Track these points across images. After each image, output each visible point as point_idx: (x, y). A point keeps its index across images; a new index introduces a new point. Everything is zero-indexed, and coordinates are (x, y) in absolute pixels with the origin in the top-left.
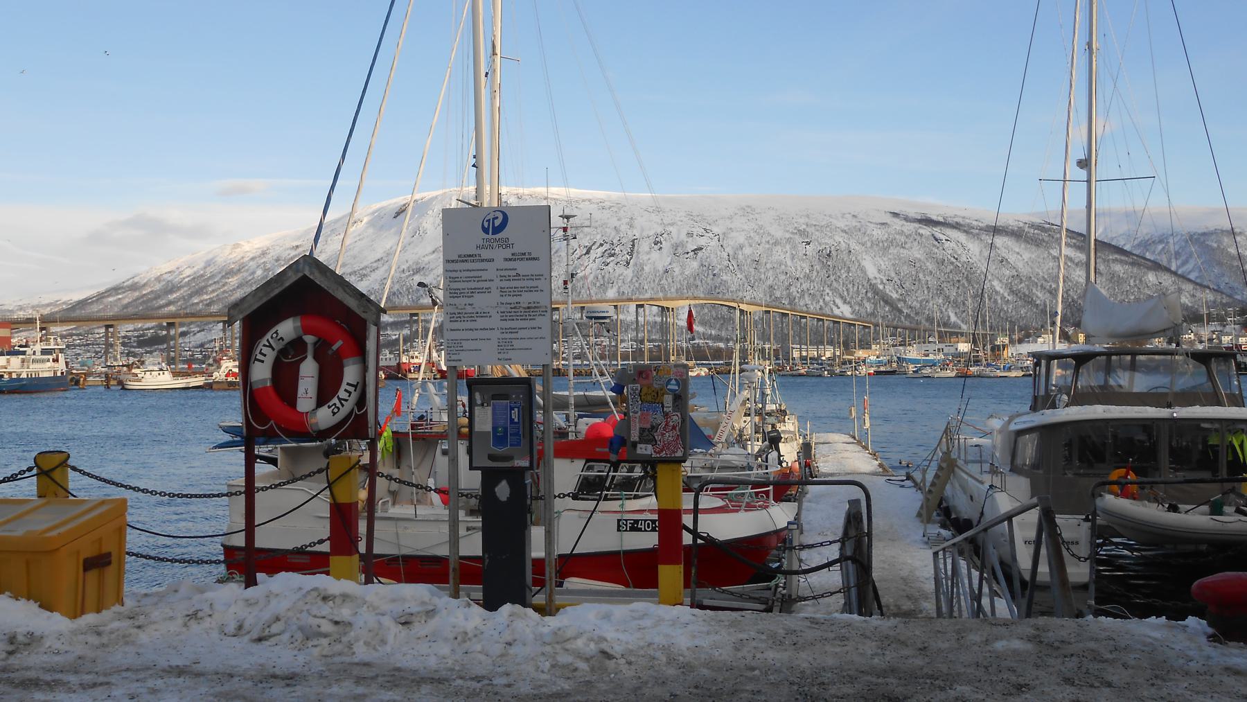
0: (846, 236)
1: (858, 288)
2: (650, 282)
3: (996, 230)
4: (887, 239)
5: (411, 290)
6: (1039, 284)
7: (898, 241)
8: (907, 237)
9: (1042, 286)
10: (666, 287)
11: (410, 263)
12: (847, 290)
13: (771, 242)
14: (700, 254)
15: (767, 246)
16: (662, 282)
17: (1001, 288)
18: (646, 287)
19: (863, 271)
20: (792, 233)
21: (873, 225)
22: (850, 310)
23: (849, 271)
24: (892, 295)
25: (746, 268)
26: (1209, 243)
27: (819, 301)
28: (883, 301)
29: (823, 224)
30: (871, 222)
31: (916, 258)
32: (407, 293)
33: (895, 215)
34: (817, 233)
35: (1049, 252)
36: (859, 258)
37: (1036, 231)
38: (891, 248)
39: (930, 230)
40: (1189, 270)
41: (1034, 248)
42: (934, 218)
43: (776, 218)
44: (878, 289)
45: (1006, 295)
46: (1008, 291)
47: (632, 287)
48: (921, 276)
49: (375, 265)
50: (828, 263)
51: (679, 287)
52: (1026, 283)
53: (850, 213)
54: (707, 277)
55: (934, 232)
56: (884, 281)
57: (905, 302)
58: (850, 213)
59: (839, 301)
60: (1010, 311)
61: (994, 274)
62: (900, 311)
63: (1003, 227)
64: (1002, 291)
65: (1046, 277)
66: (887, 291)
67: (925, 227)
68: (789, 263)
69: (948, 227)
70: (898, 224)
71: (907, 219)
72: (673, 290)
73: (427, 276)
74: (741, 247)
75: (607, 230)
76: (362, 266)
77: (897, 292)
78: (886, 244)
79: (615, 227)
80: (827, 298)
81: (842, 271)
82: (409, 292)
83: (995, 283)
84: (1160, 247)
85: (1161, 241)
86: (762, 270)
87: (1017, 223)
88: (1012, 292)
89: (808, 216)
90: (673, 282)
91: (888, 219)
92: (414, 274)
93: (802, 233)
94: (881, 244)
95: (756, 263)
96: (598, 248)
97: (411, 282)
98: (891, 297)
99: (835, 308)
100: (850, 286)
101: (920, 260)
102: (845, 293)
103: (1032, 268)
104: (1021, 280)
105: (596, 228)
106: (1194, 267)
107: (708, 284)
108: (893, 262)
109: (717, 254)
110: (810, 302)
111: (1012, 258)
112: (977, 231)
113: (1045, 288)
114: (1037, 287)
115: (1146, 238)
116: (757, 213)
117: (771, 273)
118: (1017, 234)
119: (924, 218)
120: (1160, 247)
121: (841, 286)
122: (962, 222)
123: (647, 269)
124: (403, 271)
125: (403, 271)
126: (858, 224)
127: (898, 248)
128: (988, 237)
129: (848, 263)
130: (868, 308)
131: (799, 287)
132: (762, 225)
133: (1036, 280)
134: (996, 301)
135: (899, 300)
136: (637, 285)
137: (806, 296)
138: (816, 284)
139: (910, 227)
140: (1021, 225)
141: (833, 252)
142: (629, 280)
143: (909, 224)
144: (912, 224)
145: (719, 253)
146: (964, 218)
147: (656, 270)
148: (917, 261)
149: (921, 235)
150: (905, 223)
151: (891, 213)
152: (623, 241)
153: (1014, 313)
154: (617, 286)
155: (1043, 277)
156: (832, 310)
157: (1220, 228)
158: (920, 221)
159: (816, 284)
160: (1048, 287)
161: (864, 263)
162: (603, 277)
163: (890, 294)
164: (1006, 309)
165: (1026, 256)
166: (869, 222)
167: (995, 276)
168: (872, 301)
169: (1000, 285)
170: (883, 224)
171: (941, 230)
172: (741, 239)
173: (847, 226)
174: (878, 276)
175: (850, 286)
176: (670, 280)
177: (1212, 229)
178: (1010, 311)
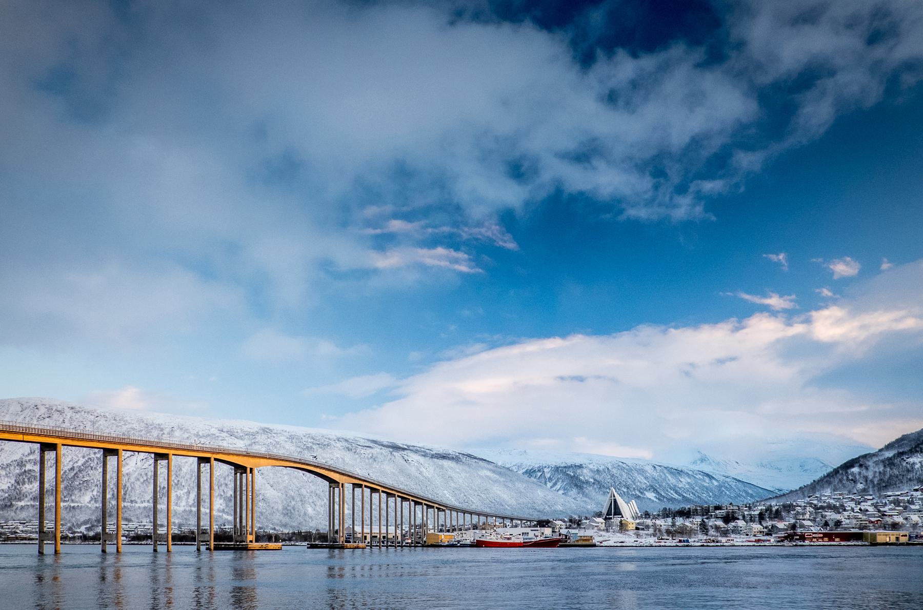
18: (183, 484)
21: (360, 447)
26: (569, 472)
30: (359, 445)
35: (477, 473)
40: (558, 489)
42: (401, 446)
58: (343, 438)
84: (539, 474)
85: (539, 471)
106: (560, 488)
115: (530, 469)
116: (274, 433)
120: (539, 474)
123: (184, 470)
136: (176, 481)
140: (457, 454)
157: (574, 464)
165: (464, 475)
173: (341, 446)
177: (569, 464)
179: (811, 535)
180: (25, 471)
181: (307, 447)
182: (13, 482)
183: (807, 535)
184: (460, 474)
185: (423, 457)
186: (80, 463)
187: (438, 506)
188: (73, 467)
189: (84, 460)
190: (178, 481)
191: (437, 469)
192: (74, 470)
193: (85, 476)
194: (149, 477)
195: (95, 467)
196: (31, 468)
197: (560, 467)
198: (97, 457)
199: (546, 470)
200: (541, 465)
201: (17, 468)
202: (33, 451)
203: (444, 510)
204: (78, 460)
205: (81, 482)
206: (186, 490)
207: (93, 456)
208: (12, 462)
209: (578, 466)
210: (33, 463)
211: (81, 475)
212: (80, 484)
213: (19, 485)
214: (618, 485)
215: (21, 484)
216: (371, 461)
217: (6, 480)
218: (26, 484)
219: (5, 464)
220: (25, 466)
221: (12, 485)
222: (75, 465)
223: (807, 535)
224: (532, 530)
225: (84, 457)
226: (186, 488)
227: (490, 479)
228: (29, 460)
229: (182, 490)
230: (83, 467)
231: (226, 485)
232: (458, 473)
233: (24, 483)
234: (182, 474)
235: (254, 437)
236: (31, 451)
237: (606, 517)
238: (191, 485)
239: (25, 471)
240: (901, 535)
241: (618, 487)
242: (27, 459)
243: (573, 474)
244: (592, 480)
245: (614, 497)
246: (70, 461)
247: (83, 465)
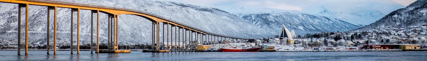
18: (85, 23)
21: (166, 5)
26: (263, 17)
40: (258, 25)
42: (186, 5)
58: (159, 1)
84: (250, 18)
85: (249, 16)
87: (210, 8)
106: (259, 24)
115: (245, 15)
120: (250, 18)
136: (81, 21)
140: (212, 9)
157: (265, 13)
165: (214, 18)
173: (158, 5)
177: (263, 13)
179: (375, 46)
180: (12, 16)
181: (142, 5)
182: (6, 21)
183: (373, 46)
185: (196, 10)
186: (37, 13)
187: (202, 33)
188: (34, 14)
189: (39, 11)
190: (83, 21)
192: (34, 16)
193: (39, 19)
194: (69, 19)
195: (44, 14)
196: (14, 15)
197: (259, 15)
198: (45, 10)
199: (253, 16)
200: (250, 14)
201: (8, 15)
202: (15, 7)
203: (205, 35)
204: (36, 11)
205: (38, 22)
206: (86, 25)
207: (43, 9)
208: (5, 12)
209: (267, 14)
210: (15, 13)
211: (37, 18)
212: (37, 22)
213: (9, 23)
214: (286, 23)
215: (10, 22)
216: (171, 12)
218: (12, 23)
219: (2, 13)
220: (12, 14)
221: (6, 23)
222: (35, 14)
223: (373, 46)
224: (246, 44)
225: (39, 10)
226: (86, 24)
227: (227, 20)
228: (14, 12)
229: (84, 25)
230: (38, 15)
231: (105, 23)
232: (212, 17)
233: (11, 22)
234: (84, 18)
236: (14, 7)
237: (280, 38)
238: (89, 23)
239: (12, 16)
240: (417, 46)
241: (286, 24)
242: (13, 11)
243: (265, 18)
244: (274, 21)
245: (284, 28)
246: (32, 12)
247: (38, 14)
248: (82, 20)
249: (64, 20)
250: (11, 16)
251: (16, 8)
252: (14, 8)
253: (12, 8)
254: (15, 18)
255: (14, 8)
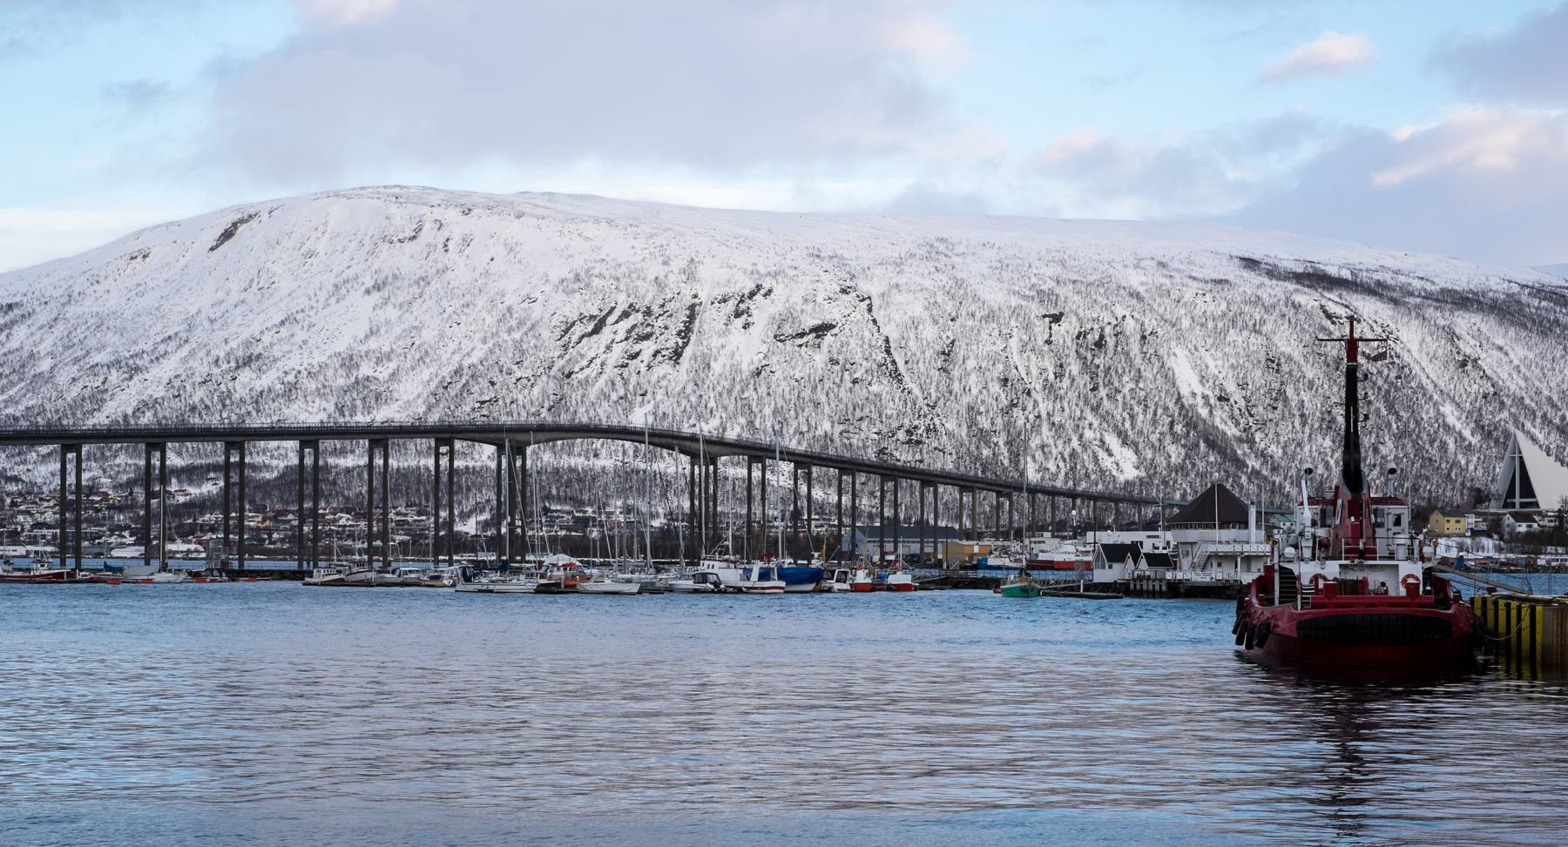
0: (1138, 306)
1: (1155, 414)
2: (721, 395)
3: (1462, 301)
4: (1224, 315)
5: (228, 402)
6: (1539, 414)
7: (1247, 318)
8: (1267, 310)
9: (1544, 416)
10: (754, 405)
11: (234, 344)
12: (1132, 417)
13: (978, 315)
14: (828, 339)
15: (970, 323)
16: (746, 395)
17: (1459, 419)
18: (712, 404)
19: (1170, 379)
20: (1026, 297)
22: (1134, 458)
23: (1139, 377)
24: (1226, 429)
25: (922, 369)
27: (1070, 440)
28: (1206, 441)
29: (1092, 279)
30: (1194, 278)
31: (1283, 354)
32: (219, 407)
33: (1250, 263)
34: (1076, 298)
36: (1161, 352)
37: (1544, 303)
38: (1232, 331)
39: (1316, 295)
41: (1535, 338)
42: (1332, 271)
43: (994, 264)
44: (1199, 416)
45: (1467, 433)
46: (1472, 425)
47: (684, 403)
48: (1290, 391)
49: (162, 348)
50: (1097, 361)
51: (779, 405)
52: (1513, 410)
53: (1153, 259)
54: (839, 386)
55: (1324, 302)
56: (1212, 401)
57: (1251, 442)
58: (1153, 259)
59: (1112, 441)
60: (1471, 467)
61: (1446, 391)
62: (1240, 464)
63: (1473, 293)
64: (1458, 426)
65: (1555, 398)
66: (1217, 422)
67: (1306, 289)
68: (1016, 359)
69: (1356, 291)
70: (1250, 282)
71: (1273, 273)
72: (768, 411)
73: (265, 373)
74: (915, 324)
75: (639, 283)
76: (135, 349)
77: (1237, 424)
78: (1220, 325)
79: (657, 278)
80: (1088, 434)
81: (1125, 379)
82: (224, 406)
83: (1448, 409)
86: (956, 373)
87: (1506, 285)
88: (1479, 427)
89: (1063, 263)
90: (769, 394)
91: (1233, 272)
92: (238, 368)
93: (1043, 296)
94: (1210, 324)
95: (943, 357)
96: (617, 322)
97: (230, 384)
98: (1225, 434)
99: (1102, 454)
100: (1138, 409)
101: (1290, 359)
102: (1128, 424)
103: (1526, 379)
104: (1502, 403)
105: (618, 279)
107: (840, 400)
108: (1232, 361)
109: (862, 338)
110: (1051, 442)
111: (1489, 360)
112: (1418, 300)
113: (1551, 422)
114: (1534, 420)
116: (957, 255)
117: (973, 379)
118: (1506, 310)
119: (1311, 271)
121: (1120, 409)
122: (1390, 282)
123: (716, 367)
124: (217, 361)
125: (217, 361)
126: (1167, 281)
127: (1246, 333)
128: (1439, 314)
129: (1138, 361)
130: (1173, 455)
131: (1030, 408)
132: (963, 280)
133: (1533, 405)
134: (1443, 446)
135: (1240, 440)
136: (693, 399)
137: (1045, 428)
138: (1066, 405)
139: (1275, 290)
140: (1515, 289)
141: (1108, 339)
142: (678, 389)
143: (1274, 282)
144: (1281, 283)
145: (867, 335)
146: (1397, 272)
147: (736, 369)
148: (1283, 360)
149: (1296, 307)
150: (1267, 281)
151: (1242, 259)
152: (670, 306)
153: (1480, 472)
154: (652, 402)
155: (1549, 399)
156: (1096, 458)
158: (1299, 278)
159: (1066, 405)
160: (1557, 421)
161: (1171, 362)
162: (626, 382)
163: (1222, 427)
164: (1463, 462)
165: (1518, 353)
166: (1190, 277)
167: (1448, 395)
168: (1183, 442)
169: (1456, 413)
170: (1220, 282)
171: (1340, 296)
172: (917, 310)
173: (1142, 284)
174: (1199, 389)
175: (1138, 409)
176: (763, 390)
178: (1471, 467)
180: (357, 382)
181: (1040, 292)
182: (331, 407)
184: (1506, 354)
186: (474, 359)
189: (486, 347)
191: (1428, 339)
193: (486, 391)
194: (631, 388)
196: (370, 373)
201: (340, 372)
204: (473, 349)
207: (506, 337)
208: (330, 357)
211: (476, 387)
212: (473, 409)
213: (344, 416)
215: (347, 413)
217: (316, 405)
218: (359, 414)
219: (316, 366)
221: (330, 415)
222: (466, 363)
224: (1149, 537)
225: (484, 341)
226: (718, 416)
230: (481, 367)
231: (817, 405)
234: (712, 378)
235: (898, 269)
237: (1505, 501)
238: (731, 407)
242: (364, 348)
245: (1520, 453)
246: (453, 353)
248: (698, 393)
249: (607, 397)
250: (355, 374)
251: (378, 330)
252: (368, 332)
253: (361, 336)
254: (371, 391)
255: (372, 332)
